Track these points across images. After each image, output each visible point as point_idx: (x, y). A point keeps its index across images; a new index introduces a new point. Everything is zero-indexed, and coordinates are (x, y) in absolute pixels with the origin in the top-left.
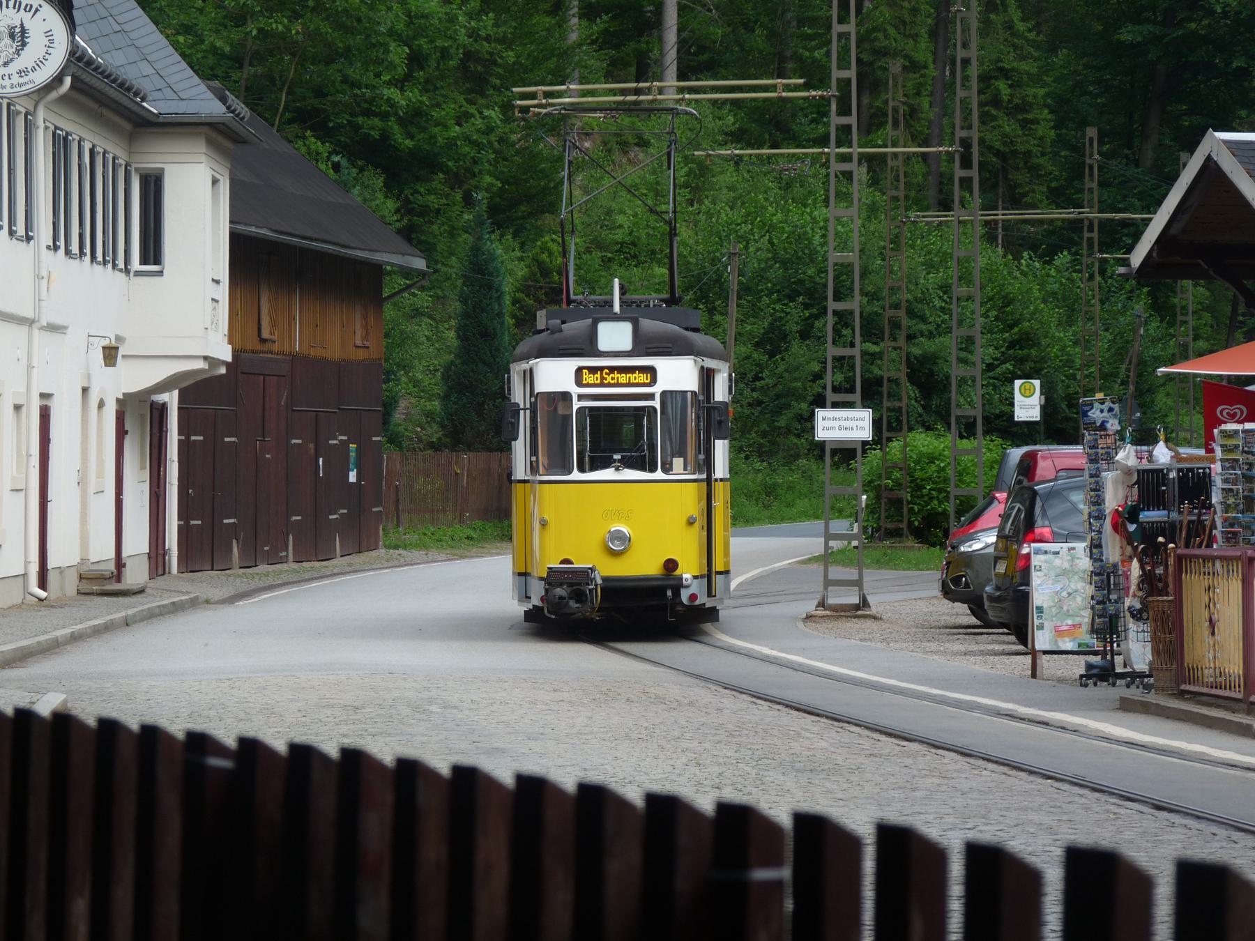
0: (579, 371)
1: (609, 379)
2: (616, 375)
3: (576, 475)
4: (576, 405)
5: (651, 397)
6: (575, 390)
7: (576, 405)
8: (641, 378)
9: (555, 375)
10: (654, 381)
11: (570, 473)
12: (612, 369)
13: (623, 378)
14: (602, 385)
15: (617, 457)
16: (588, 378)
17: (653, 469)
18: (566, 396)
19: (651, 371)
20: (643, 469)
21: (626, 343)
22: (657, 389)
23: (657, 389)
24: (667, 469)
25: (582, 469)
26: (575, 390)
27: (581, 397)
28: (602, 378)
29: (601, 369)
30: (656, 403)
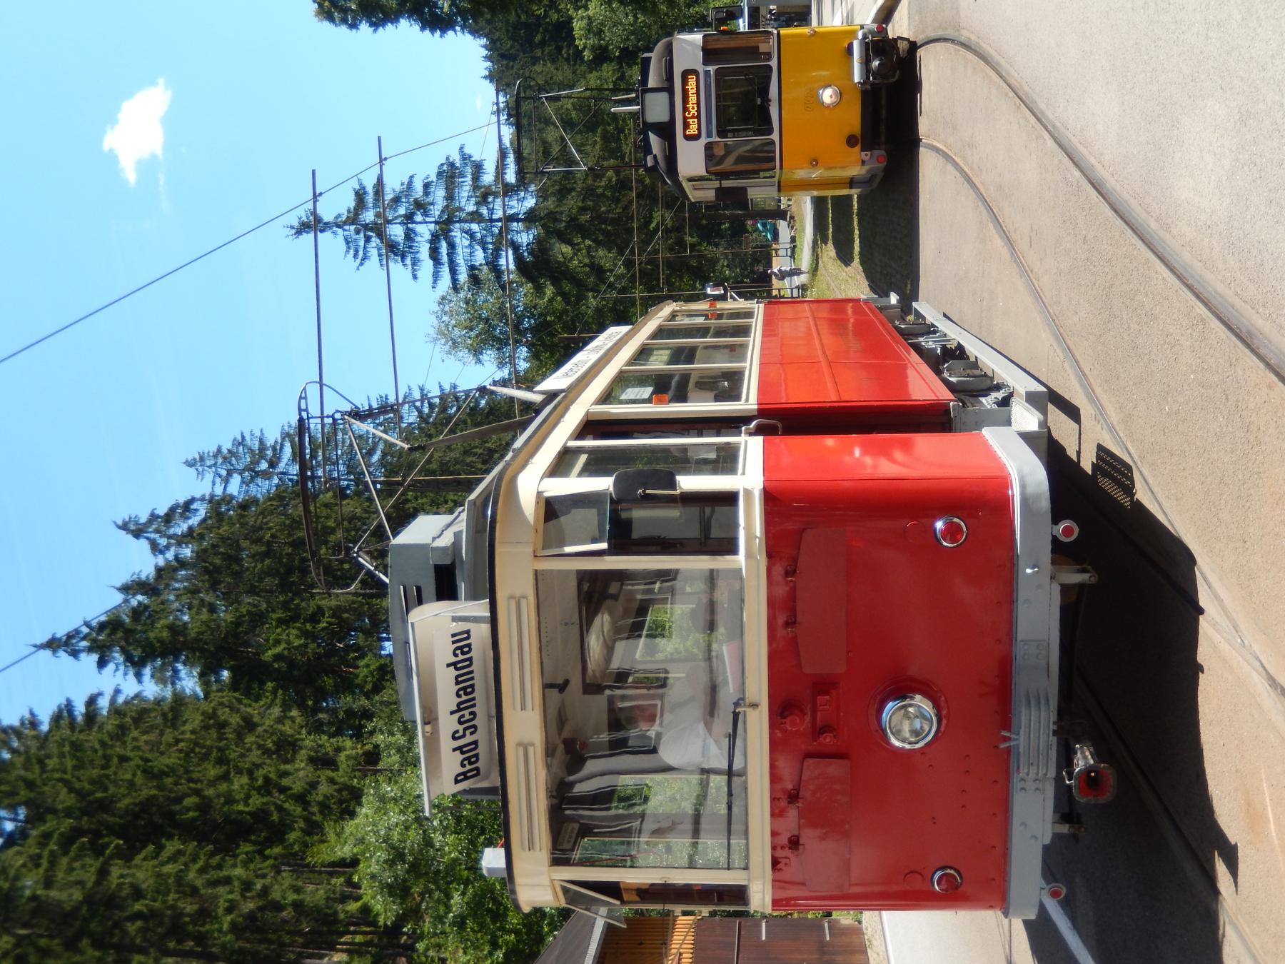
1: (693, 111)
2: (690, 105)
3: (775, 137)
5: (707, 73)
6: (704, 140)
8: (692, 84)
9: (691, 160)
10: (694, 72)
11: (773, 142)
12: (685, 109)
13: (693, 99)
14: (698, 117)
15: (759, 101)
16: (693, 130)
17: (770, 68)
18: (708, 147)
19: (686, 74)
20: (768, 79)
21: (664, 97)
24: (768, 56)
25: (770, 132)
26: (704, 140)
27: (709, 135)
28: (693, 117)
29: (685, 118)
30: (712, 69)
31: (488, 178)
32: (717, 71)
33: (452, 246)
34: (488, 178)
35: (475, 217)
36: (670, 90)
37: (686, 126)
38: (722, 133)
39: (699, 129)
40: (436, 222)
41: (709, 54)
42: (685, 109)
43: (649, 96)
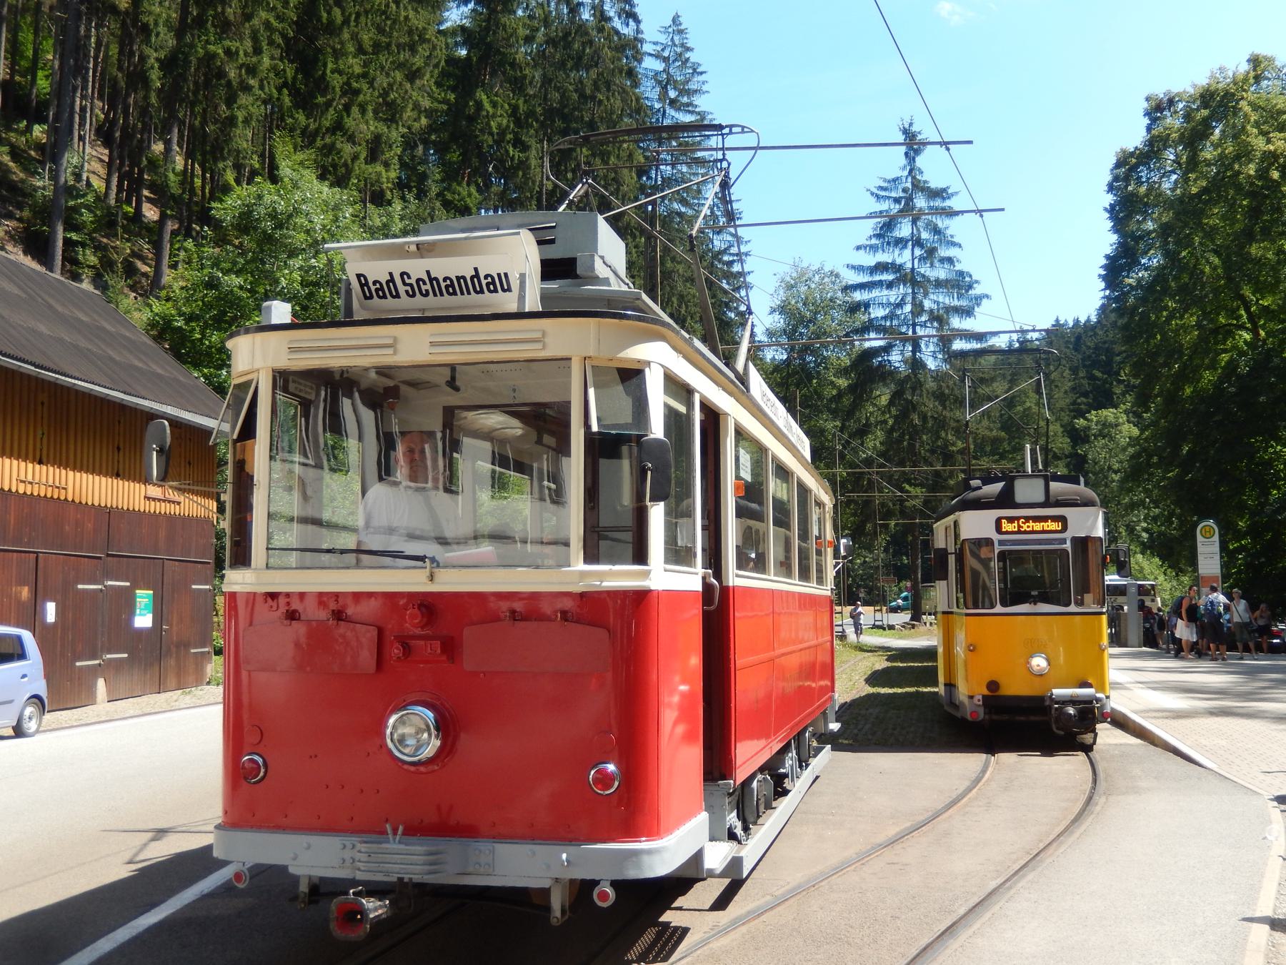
0: (998, 522)
1: (1025, 527)
2: (1031, 524)
3: (999, 609)
4: (997, 549)
5: (1063, 541)
6: (996, 537)
7: (997, 549)
9: (976, 524)
10: (1065, 529)
11: (992, 607)
12: (1027, 519)
13: (1038, 526)
14: (1019, 532)
15: (1034, 593)
16: (1006, 526)
17: (1068, 604)
18: (989, 542)
19: (1062, 519)
20: (1059, 604)
21: (1040, 498)
22: (1068, 535)
23: (1068, 535)
24: (1080, 603)
25: (1004, 604)
26: (996, 537)
27: (1001, 543)
28: (1019, 526)
29: (1018, 518)
30: (1068, 546)
31: (956, 322)
32: (1065, 551)
33: (890, 285)
34: (956, 322)
35: (918, 309)
36: (1047, 504)
37: (1011, 520)
38: (1002, 556)
39: (1007, 533)
40: (913, 269)
41: (1082, 544)
42: (1027, 519)
43: (1041, 482)
